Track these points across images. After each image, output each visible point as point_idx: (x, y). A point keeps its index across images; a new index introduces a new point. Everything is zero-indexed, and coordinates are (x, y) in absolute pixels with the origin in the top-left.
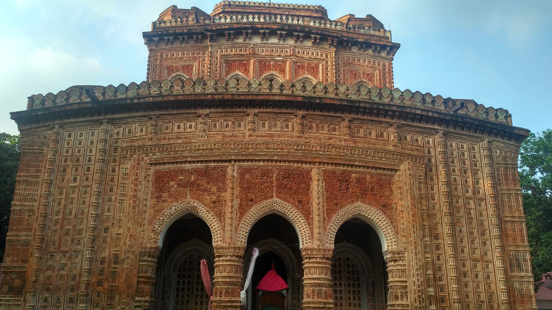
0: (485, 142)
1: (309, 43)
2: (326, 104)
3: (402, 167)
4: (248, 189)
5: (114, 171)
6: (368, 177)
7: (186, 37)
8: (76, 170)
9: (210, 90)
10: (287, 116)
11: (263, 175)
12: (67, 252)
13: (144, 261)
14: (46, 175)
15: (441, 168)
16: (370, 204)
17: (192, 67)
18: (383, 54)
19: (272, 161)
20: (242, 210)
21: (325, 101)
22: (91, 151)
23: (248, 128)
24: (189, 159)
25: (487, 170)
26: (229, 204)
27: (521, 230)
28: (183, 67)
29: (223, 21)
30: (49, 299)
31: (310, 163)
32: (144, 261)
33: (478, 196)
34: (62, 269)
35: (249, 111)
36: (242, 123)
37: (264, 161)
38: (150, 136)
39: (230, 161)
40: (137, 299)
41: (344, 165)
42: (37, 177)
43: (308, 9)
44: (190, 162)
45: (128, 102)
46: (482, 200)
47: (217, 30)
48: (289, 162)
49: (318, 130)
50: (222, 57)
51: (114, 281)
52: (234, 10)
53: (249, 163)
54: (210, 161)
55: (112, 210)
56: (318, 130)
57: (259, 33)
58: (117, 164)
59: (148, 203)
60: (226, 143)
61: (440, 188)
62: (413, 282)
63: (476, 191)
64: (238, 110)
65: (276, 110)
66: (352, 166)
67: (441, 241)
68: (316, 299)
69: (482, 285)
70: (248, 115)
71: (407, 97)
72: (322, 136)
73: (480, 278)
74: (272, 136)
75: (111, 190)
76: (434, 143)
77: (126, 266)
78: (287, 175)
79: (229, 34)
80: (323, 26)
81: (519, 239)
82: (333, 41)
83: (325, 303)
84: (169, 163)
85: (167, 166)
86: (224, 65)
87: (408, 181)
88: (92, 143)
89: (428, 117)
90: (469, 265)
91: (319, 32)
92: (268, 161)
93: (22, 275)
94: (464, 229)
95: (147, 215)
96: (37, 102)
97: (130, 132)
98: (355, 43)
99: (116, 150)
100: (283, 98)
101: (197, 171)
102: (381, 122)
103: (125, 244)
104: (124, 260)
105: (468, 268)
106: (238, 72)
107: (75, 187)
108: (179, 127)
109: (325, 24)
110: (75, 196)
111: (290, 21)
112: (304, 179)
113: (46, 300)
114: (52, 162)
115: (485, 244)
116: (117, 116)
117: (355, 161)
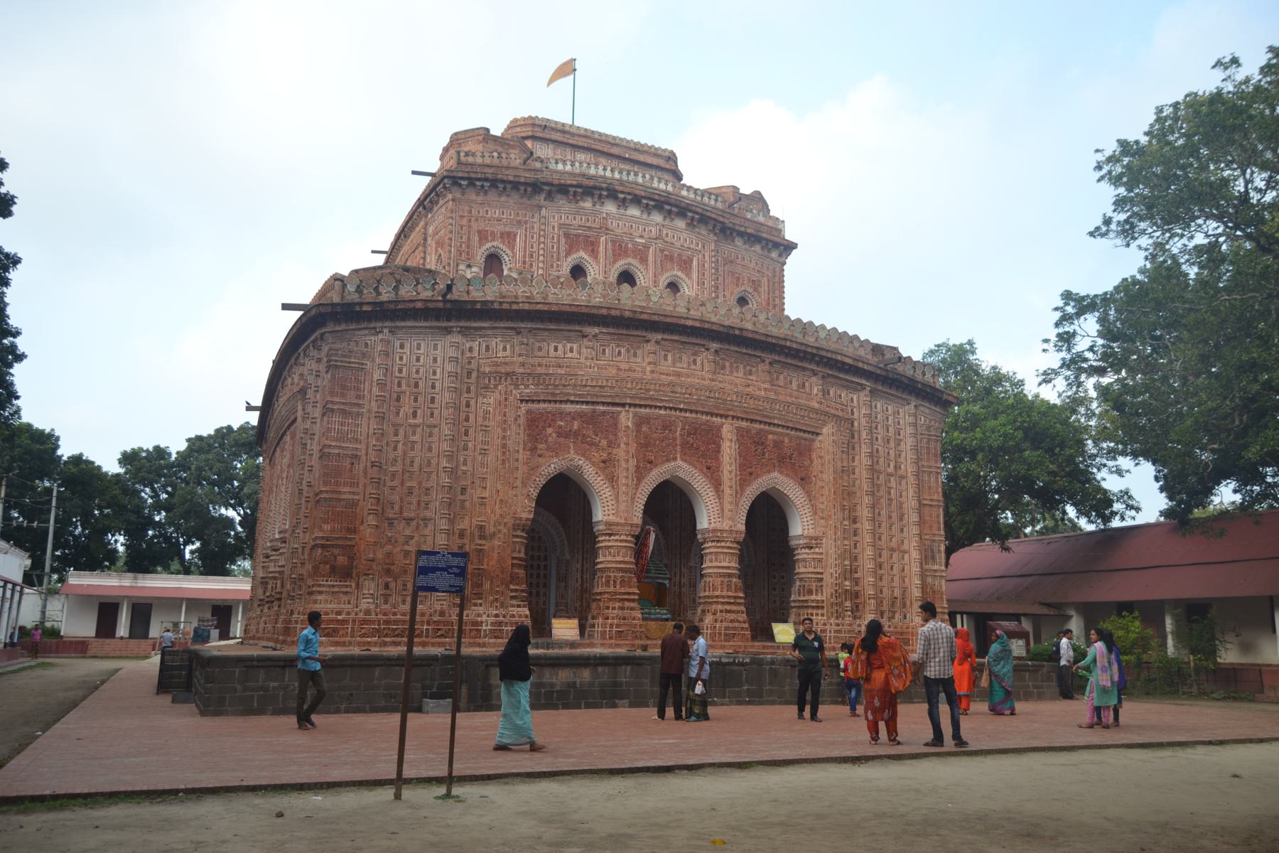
0: (912, 406)
1: (681, 224)
2: (746, 338)
3: (825, 431)
4: (647, 445)
5: (468, 405)
6: (786, 440)
7: (509, 186)
8: (416, 400)
9: (597, 300)
10: (696, 348)
11: (665, 428)
12: (412, 519)
13: (517, 536)
14: (373, 404)
15: (864, 435)
16: (788, 475)
17: (515, 235)
18: (774, 255)
19: (676, 409)
20: (640, 476)
21: (745, 334)
22: (434, 373)
23: (647, 360)
24: (572, 398)
25: (910, 441)
26: (624, 465)
27: (938, 516)
28: (502, 234)
29: (560, 167)
30: (392, 585)
31: (722, 416)
32: (517, 536)
33: (900, 472)
34: (407, 543)
35: (650, 335)
36: (639, 352)
37: (666, 408)
38: (521, 359)
39: (623, 405)
40: (512, 587)
41: (761, 422)
42: (358, 405)
43: (655, 152)
44: (572, 402)
45: (496, 306)
46: (902, 477)
47: (560, 185)
48: (697, 412)
49: (731, 372)
50: (561, 226)
51: (481, 562)
52: (548, 136)
53: (648, 410)
54: (598, 403)
55: (469, 463)
56: (731, 372)
57: (616, 198)
58: (472, 395)
59: (521, 457)
60: (622, 380)
61: (862, 460)
62: (831, 574)
63: (897, 467)
64: (636, 333)
65: (684, 339)
66: (770, 424)
67: (858, 525)
68: (724, 593)
69: (896, 579)
70: (648, 341)
71: (834, 338)
72: (737, 381)
73: (895, 571)
74: (678, 375)
75: (466, 434)
76: (858, 402)
77: (497, 543)
78: (694, 430)
79: (575, 193)
80: (699, 198)
81: (935, 526)
82: (714, 226)
83: (735, 597)
84: (544, 401)
85: (542, 405)
86: (563, 240)
87: (831, 449)
88: (435, 360)
89: (857, 368)
90: (885, 553)
91: (699, 210)
92: (671, 409)
93: (349, 550)
94: (883, 512)
95: (519, 474)
96: (351, 288)
97: (487, 348)
98: (741, 234)
99: (469, 374)
100: (697, 324)
101: (581, 415)
102: (804, 369)
103: (493, 511)
104: (494, 534)
105: (883, 559)
106: (582, 254)
107: (416, 426)
108: (556, 349)
109: (703, 196)
110: (416, 438)
111: (655, 184)
112: (713, 437)
113: (387, 586)
114: (382, 385)
115: (902, 530)
116: (474, 325)
117: (774, 418)
